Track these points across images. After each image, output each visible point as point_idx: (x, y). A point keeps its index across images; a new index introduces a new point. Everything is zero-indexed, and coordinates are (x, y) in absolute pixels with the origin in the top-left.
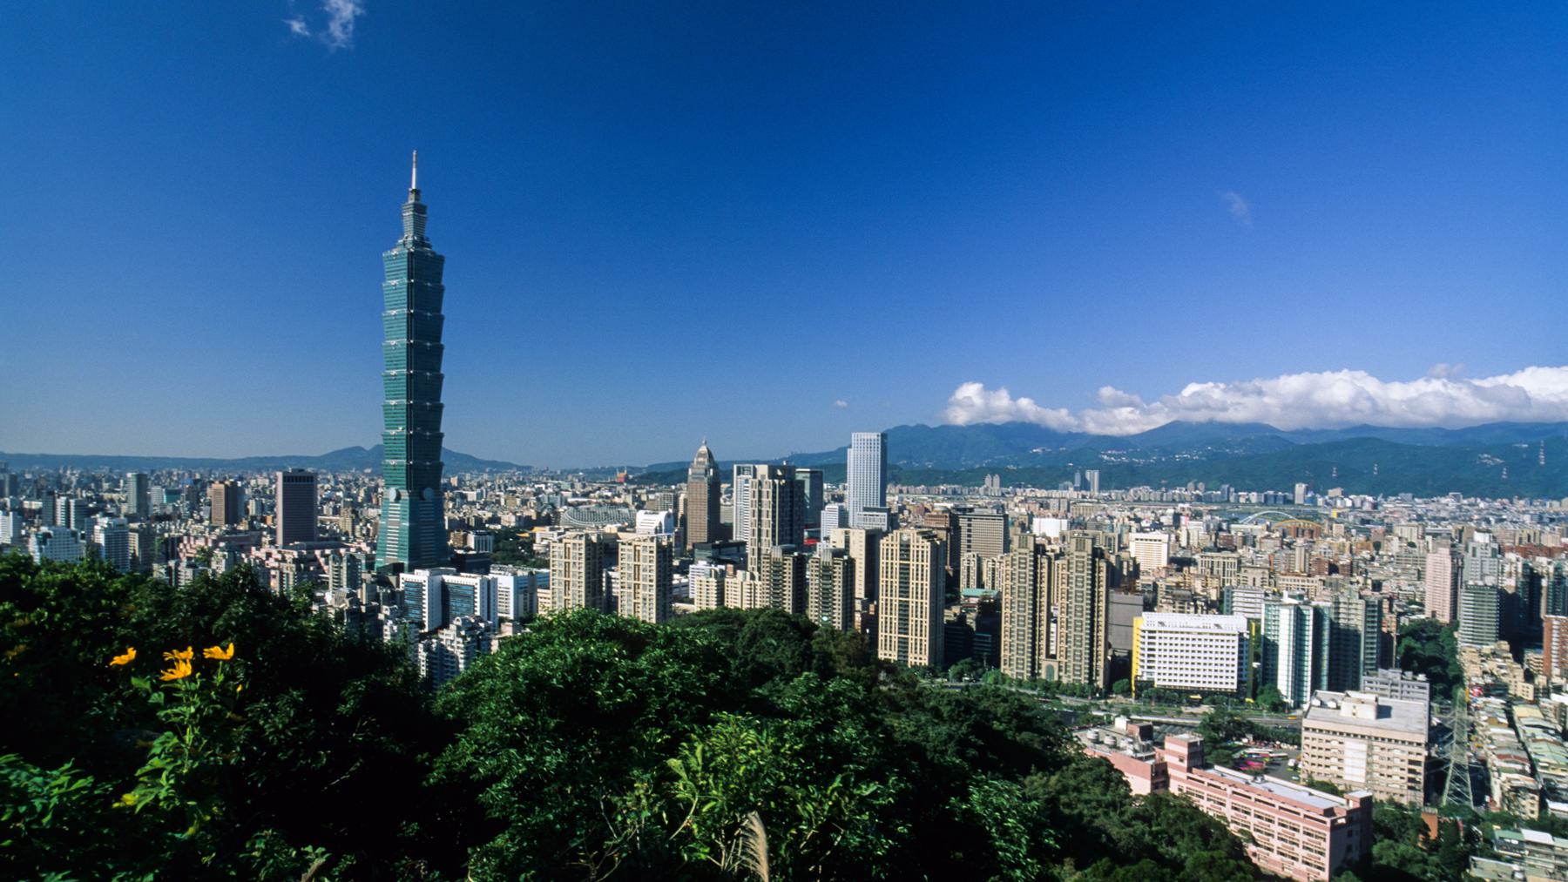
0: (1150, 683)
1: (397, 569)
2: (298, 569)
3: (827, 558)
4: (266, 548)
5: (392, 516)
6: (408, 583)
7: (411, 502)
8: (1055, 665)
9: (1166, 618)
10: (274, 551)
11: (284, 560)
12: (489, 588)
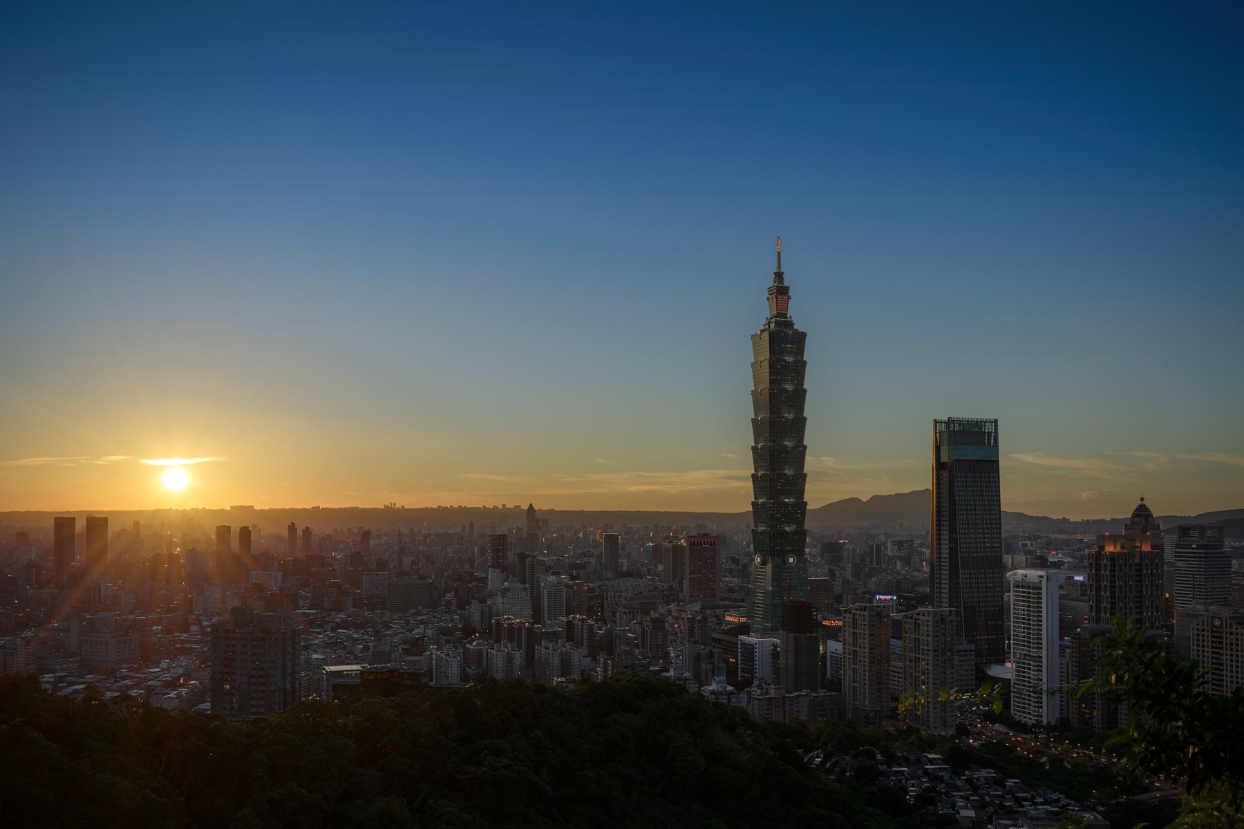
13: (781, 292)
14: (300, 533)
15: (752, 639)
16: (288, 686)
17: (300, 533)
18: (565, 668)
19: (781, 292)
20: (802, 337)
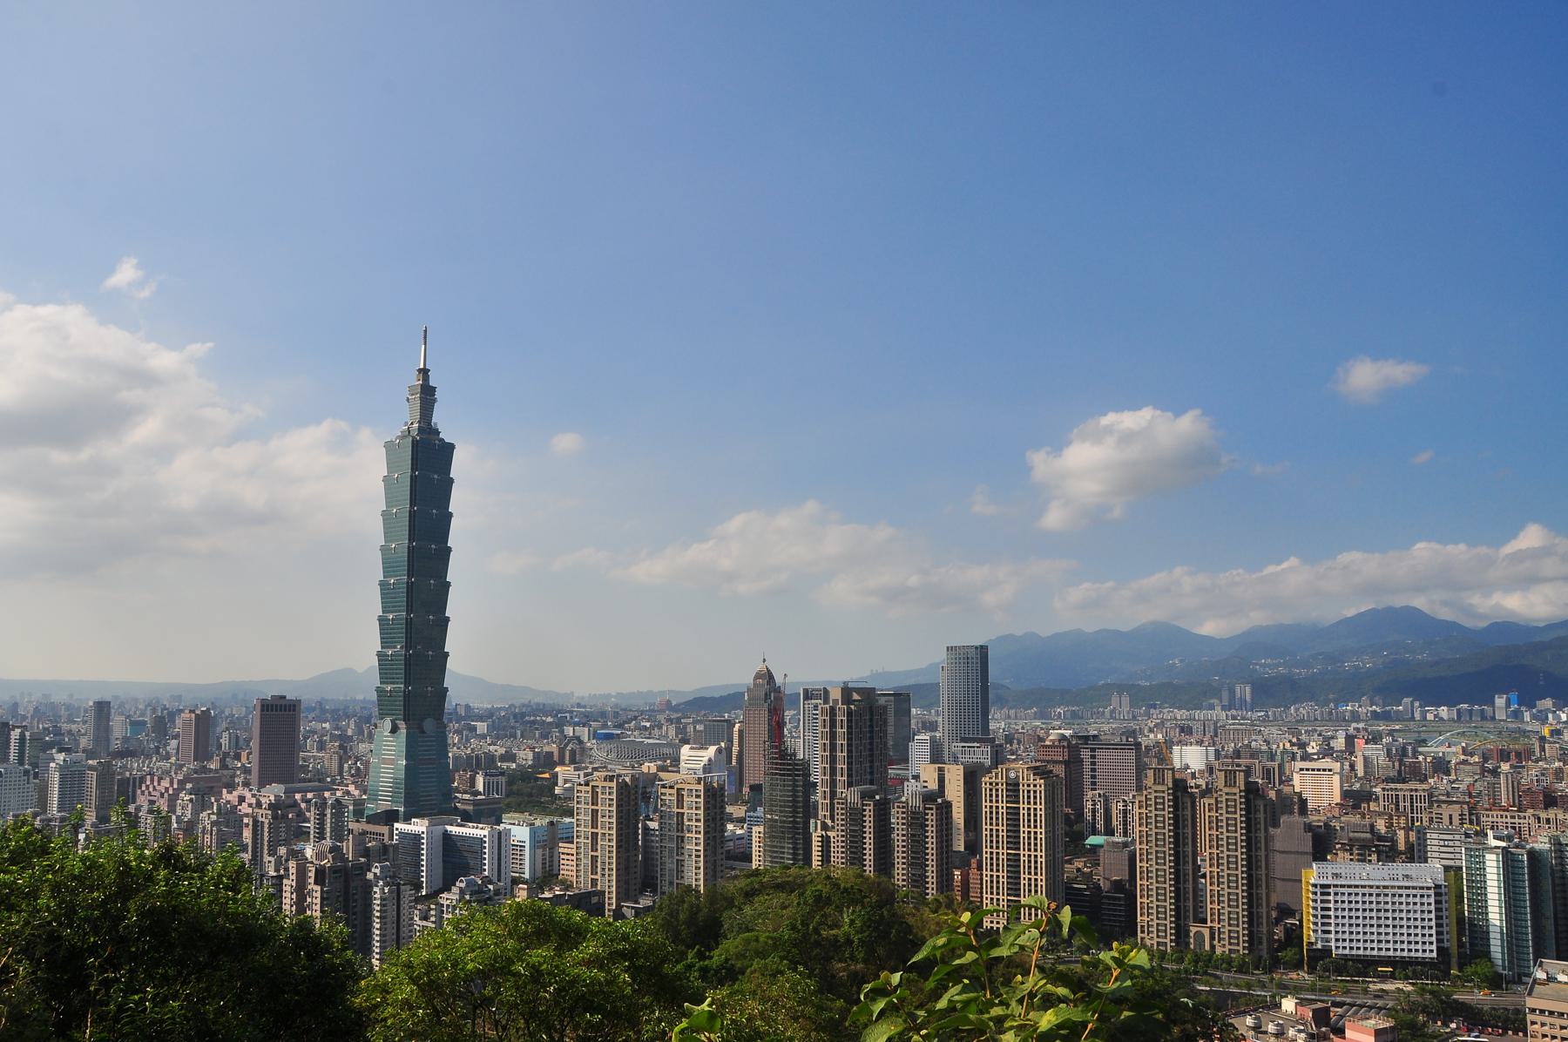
0: (1326, 952)
1: (390, 817)
2: (275, 817)
3: (917, 803)
4: (240, 791)
5: (388, 755)
6: (403, 835)
8: (1206, 932)
9: (1344, 869)
10: (248, 795)
11: (259, 805)
12: (500, 839)
19: (427, 395)
20: (451, 447)
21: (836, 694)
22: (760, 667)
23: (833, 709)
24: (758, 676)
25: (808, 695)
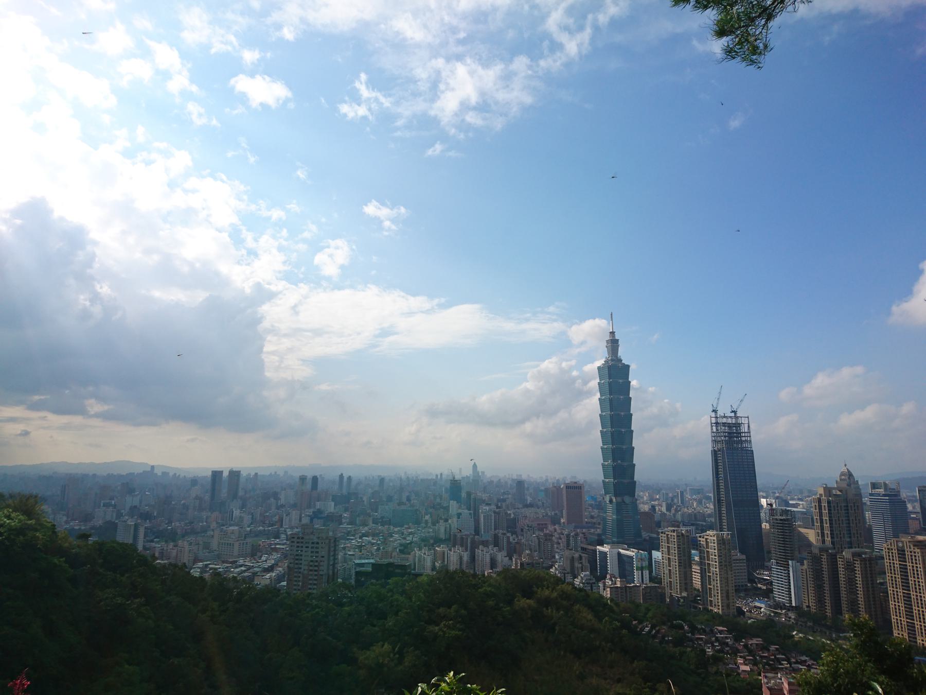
7: (617, 503)
13: (613, 344)
14: (345, 479)
15: (605, 548)
16: (331, 572)
17: (345, 479)
18: (493, 564)
19: (613, 344)
20: (628, 366)
21: (821, 491)
22: (844, 469)
23: (819, 501)
24: (842, 474)
25: (874, 486)
